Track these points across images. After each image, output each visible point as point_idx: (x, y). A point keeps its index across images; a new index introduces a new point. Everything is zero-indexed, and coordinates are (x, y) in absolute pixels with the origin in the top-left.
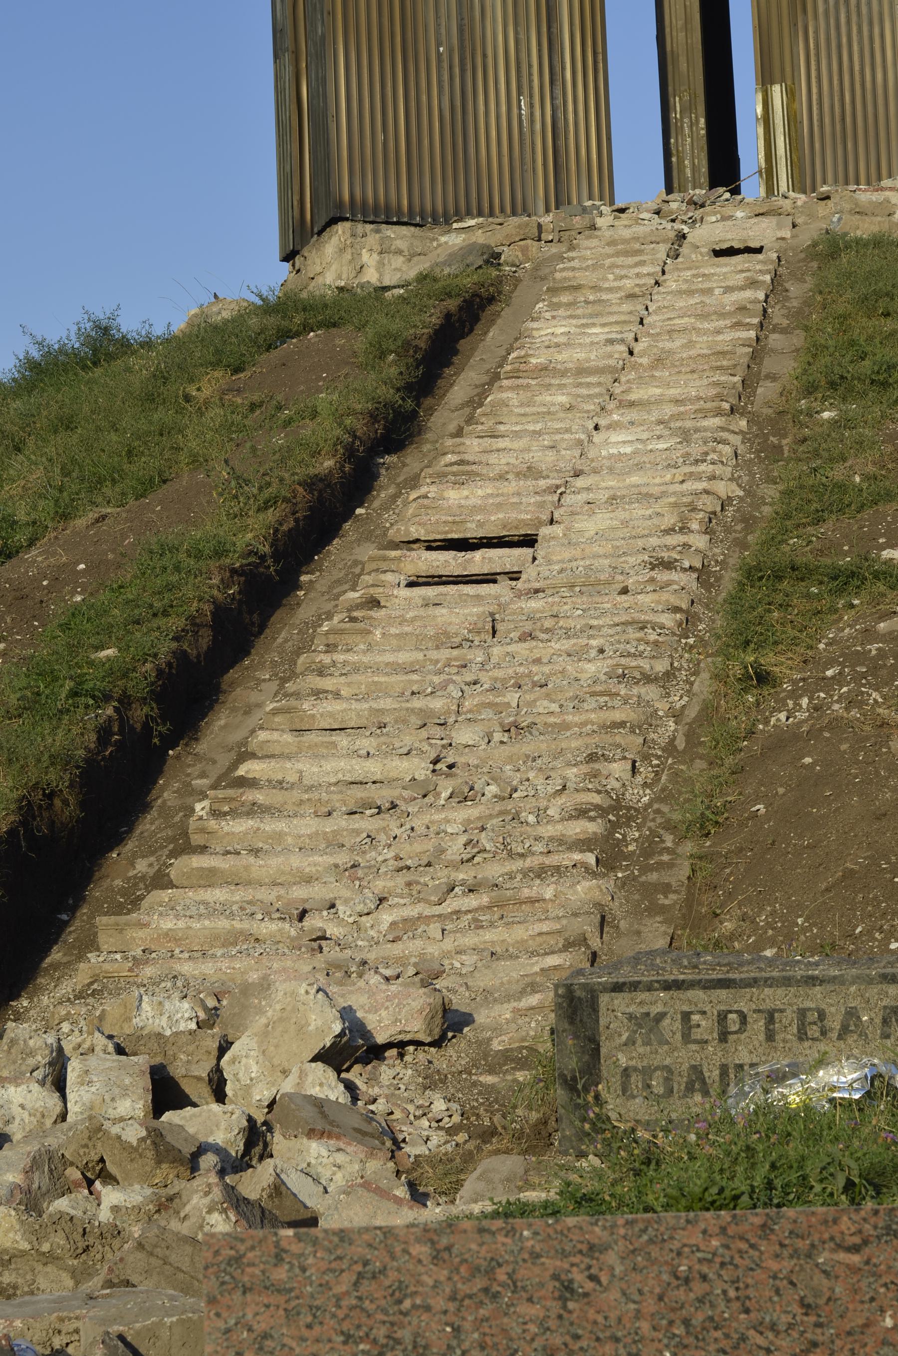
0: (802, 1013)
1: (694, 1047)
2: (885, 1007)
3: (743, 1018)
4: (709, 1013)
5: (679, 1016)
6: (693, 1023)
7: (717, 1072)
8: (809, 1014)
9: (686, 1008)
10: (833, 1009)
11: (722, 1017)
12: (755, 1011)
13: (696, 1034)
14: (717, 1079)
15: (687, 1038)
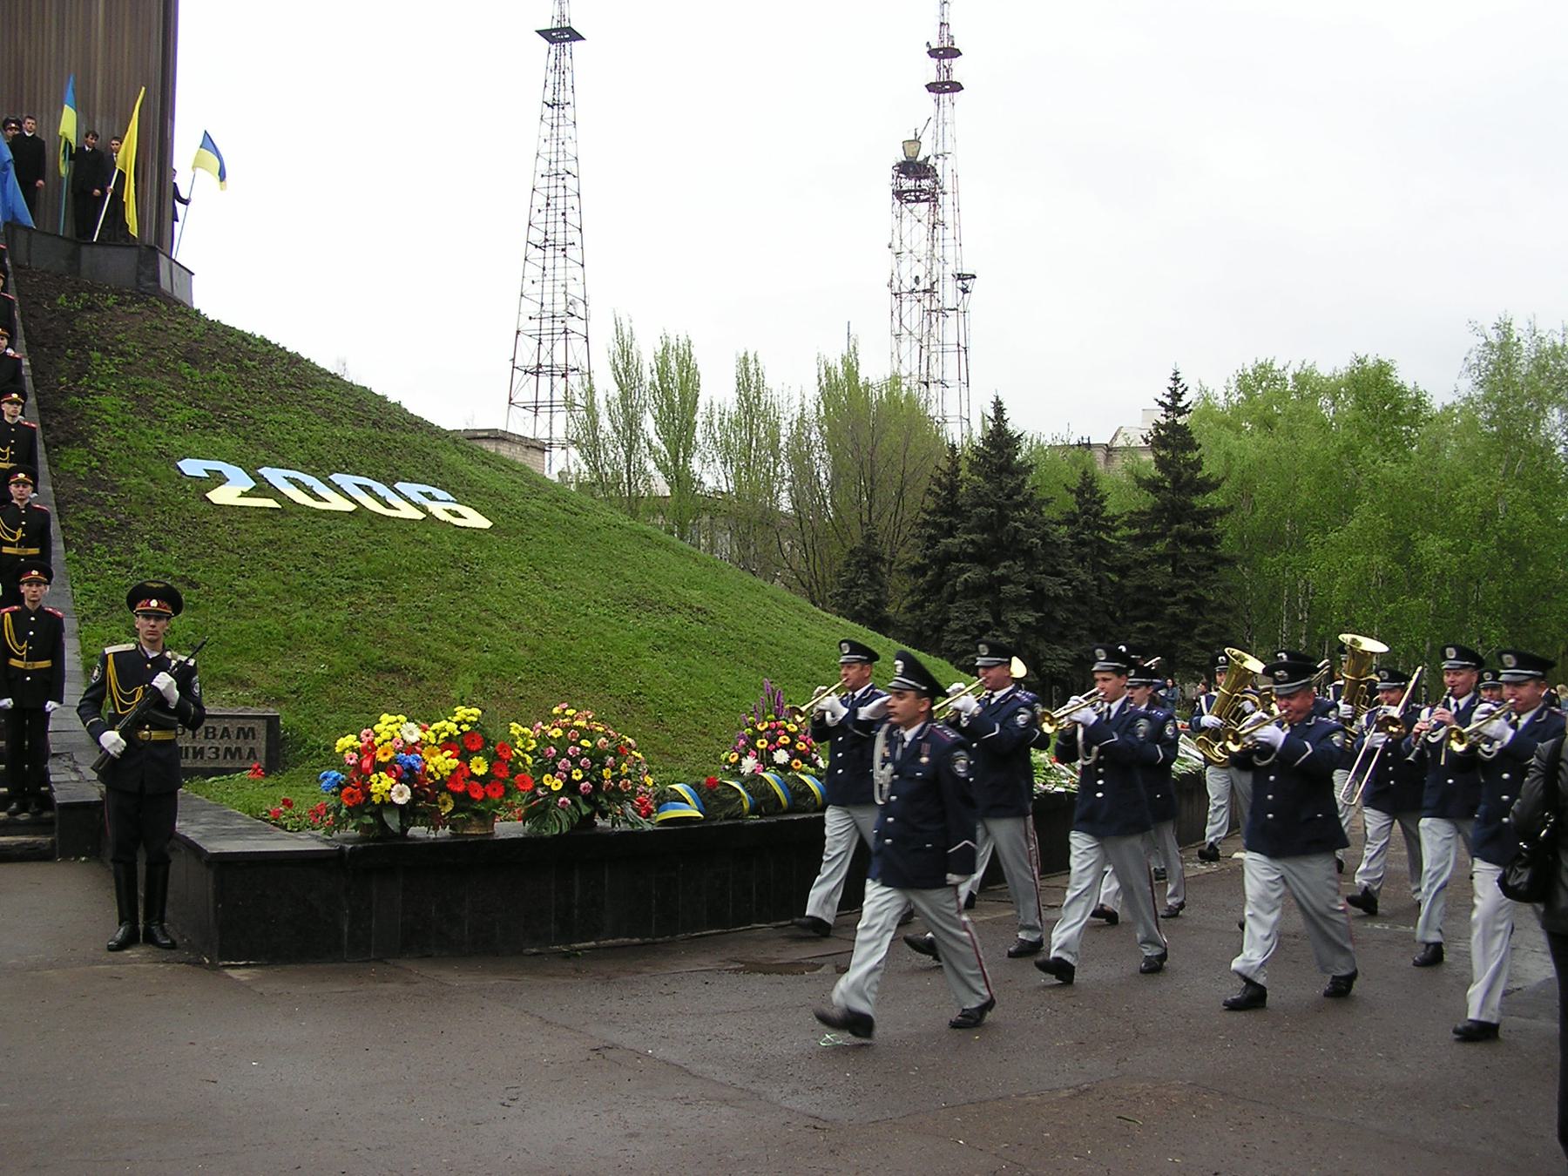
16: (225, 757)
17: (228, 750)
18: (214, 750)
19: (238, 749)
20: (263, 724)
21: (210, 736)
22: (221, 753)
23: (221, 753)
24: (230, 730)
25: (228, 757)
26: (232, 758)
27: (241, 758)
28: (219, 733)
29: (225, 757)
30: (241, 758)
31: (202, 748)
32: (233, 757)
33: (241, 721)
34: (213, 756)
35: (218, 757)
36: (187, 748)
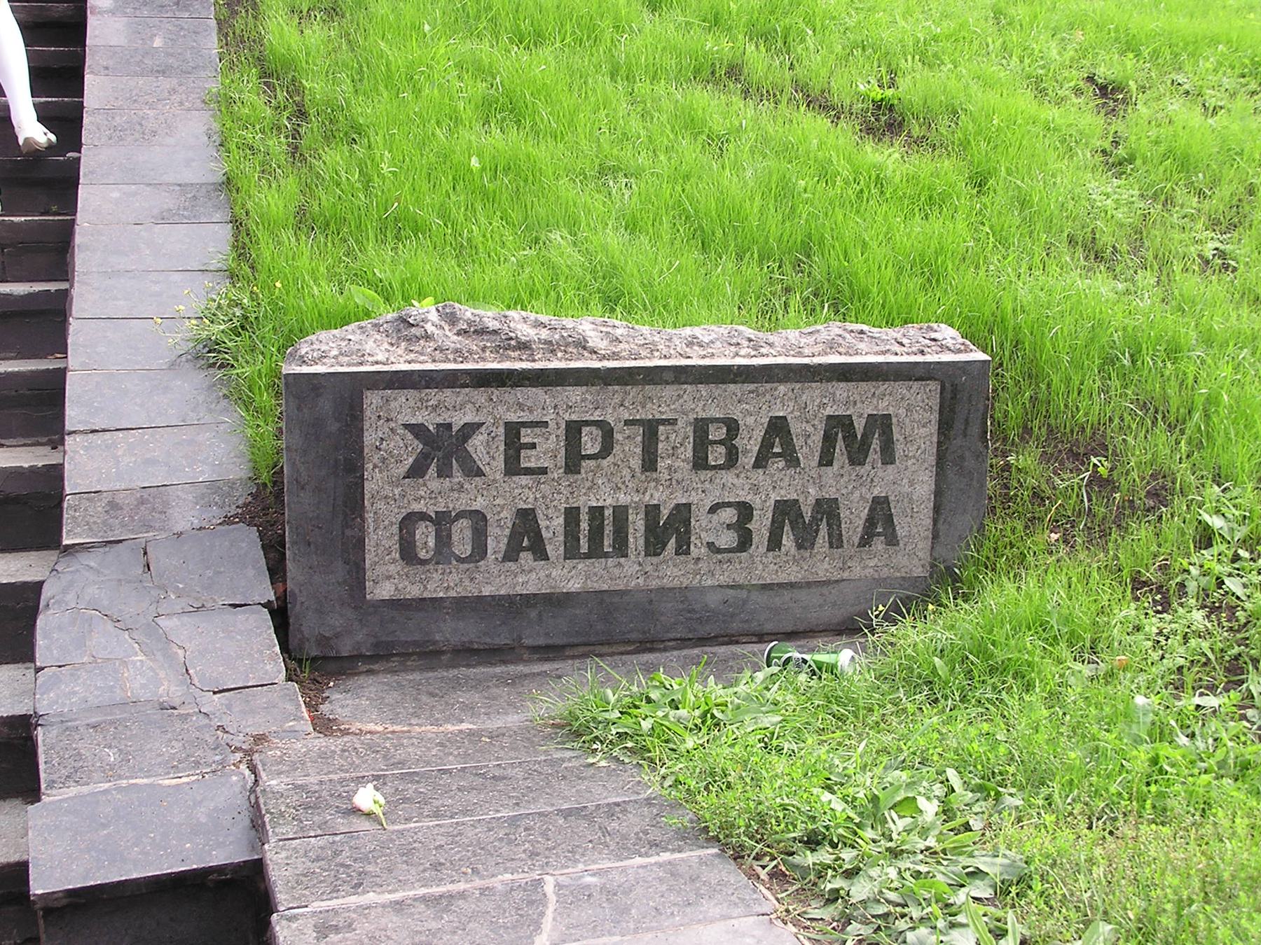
0: (701, 427)
1: (525, 480)
2: (829, 417)
3: (607, 433)
4: (552, 425)
5: (502, 430)
6: (524, 440)
7: (561, 520)
8: (711, 428)
9: (513, 417)
10: (750, 420)
11: (573, 430)
12: (627, 423)
13: (529, 460)
14: (561, 530)
15: (513, 467)
16: (774, 543)
17: (786, 511)
18: (729, 515)
19: (828, 509)
20: (925, 398)
21: (717, 455)
22: (760, 526)
23: (760, 526)
24: (795, 428)
25: (788, 541)
26: (800, 547)
27: (836, 541)
28: (750, 443)
29: (774, 543)
30: (836, 541)
31: (682, 513)
32: (805, 542)
33: (841, 390)
34: (728, 539)
35: (745, 542)
36: (621, 513)
